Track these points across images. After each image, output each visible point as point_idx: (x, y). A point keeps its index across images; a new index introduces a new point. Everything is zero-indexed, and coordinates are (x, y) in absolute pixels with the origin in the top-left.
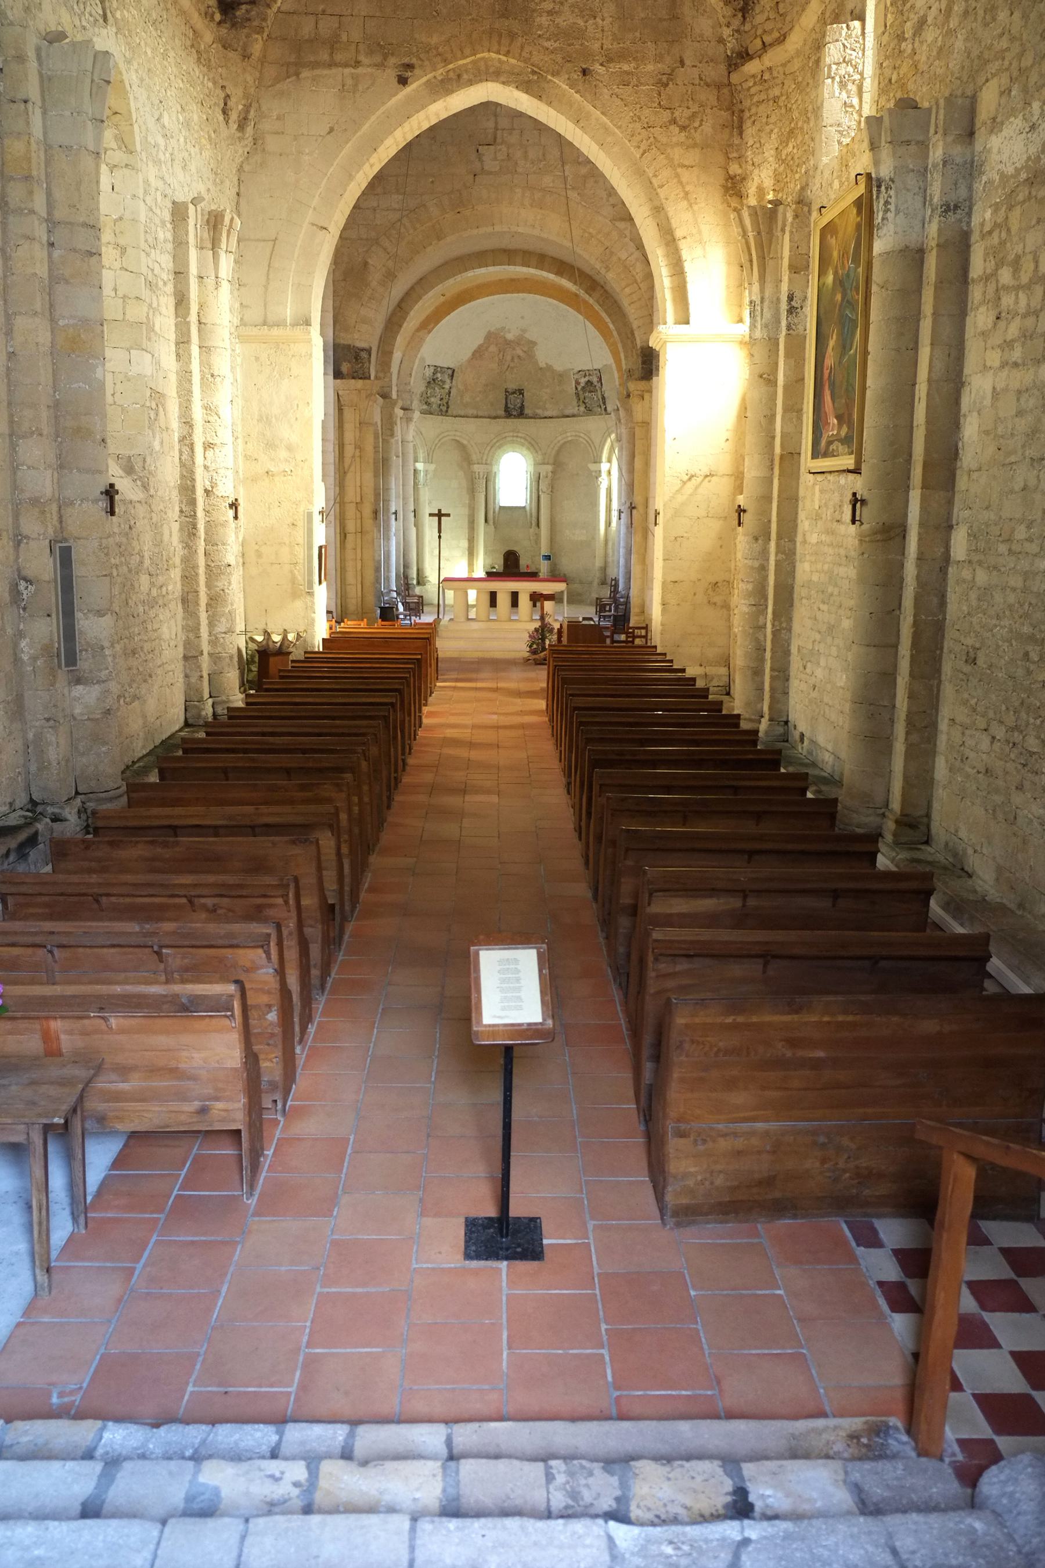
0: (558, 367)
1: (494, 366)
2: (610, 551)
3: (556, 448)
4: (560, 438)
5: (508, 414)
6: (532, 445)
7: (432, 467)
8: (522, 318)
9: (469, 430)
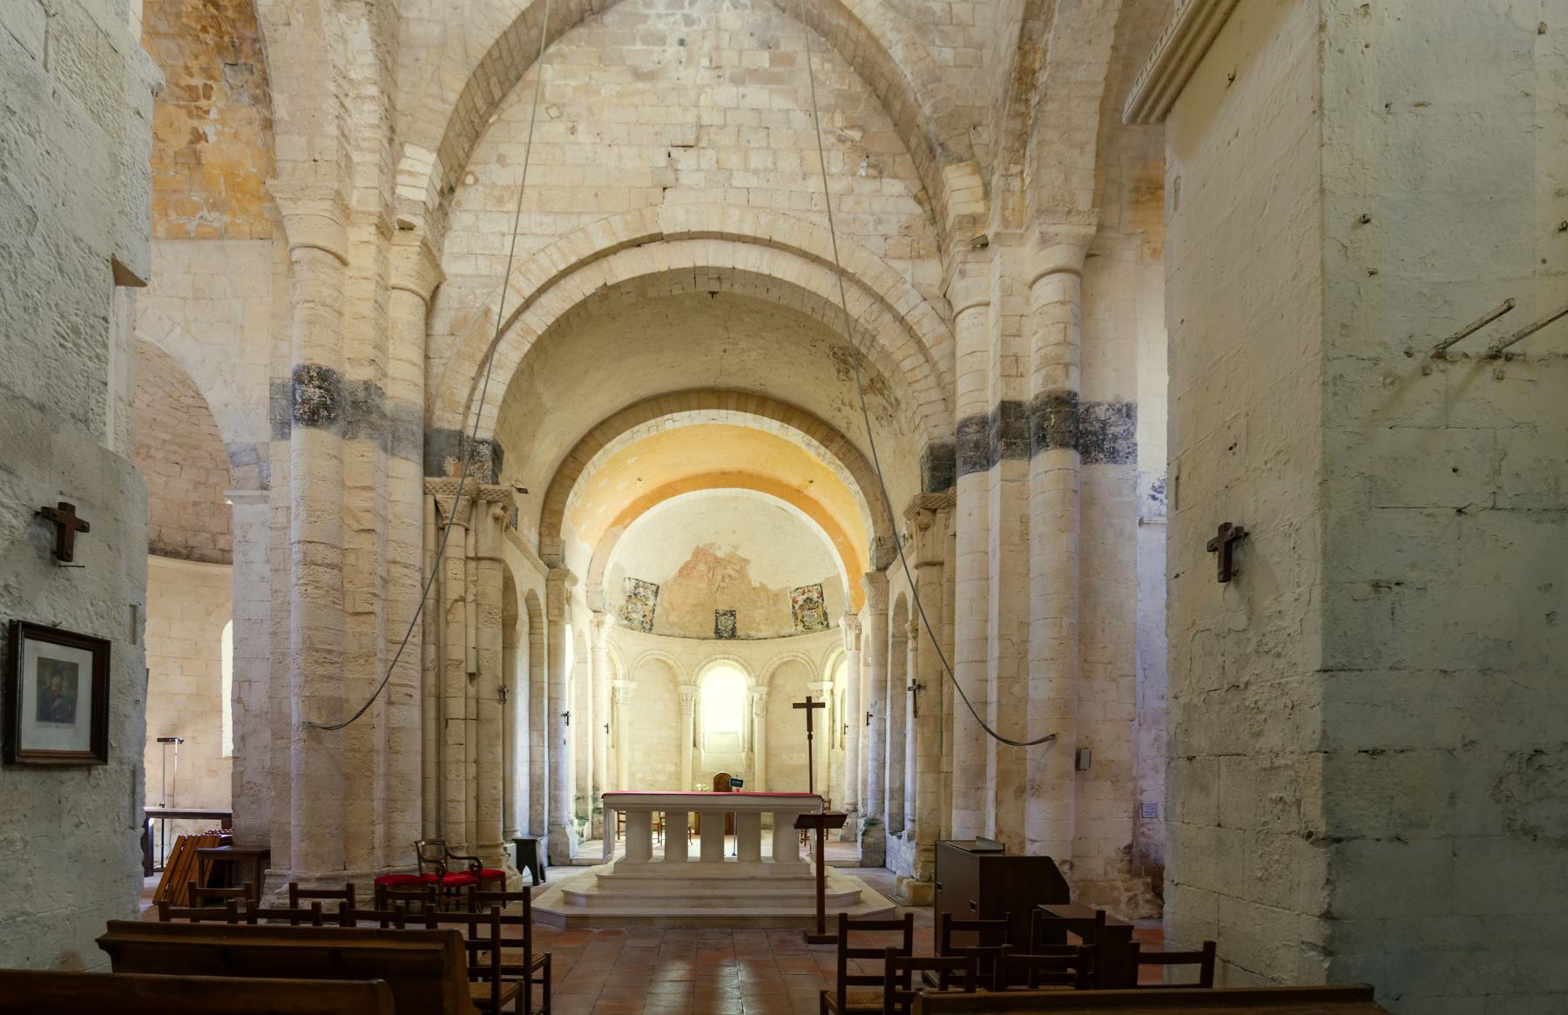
0: (773, 586)
1: (704, 586)
2: (833, 774)
3: (771, 670)
4: (775, 659)
5: (719, 635)
6: (747, 666)
7: (634, 685)
8: (734, 532)
9: (675, 649)
